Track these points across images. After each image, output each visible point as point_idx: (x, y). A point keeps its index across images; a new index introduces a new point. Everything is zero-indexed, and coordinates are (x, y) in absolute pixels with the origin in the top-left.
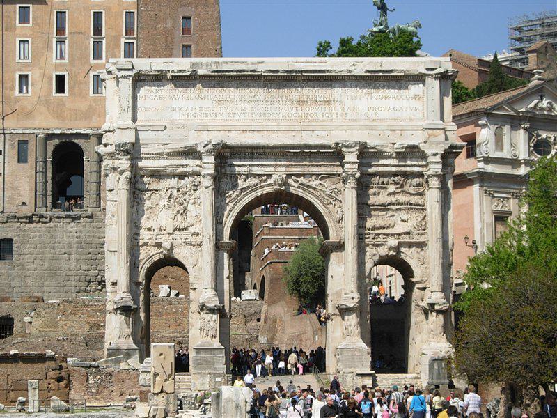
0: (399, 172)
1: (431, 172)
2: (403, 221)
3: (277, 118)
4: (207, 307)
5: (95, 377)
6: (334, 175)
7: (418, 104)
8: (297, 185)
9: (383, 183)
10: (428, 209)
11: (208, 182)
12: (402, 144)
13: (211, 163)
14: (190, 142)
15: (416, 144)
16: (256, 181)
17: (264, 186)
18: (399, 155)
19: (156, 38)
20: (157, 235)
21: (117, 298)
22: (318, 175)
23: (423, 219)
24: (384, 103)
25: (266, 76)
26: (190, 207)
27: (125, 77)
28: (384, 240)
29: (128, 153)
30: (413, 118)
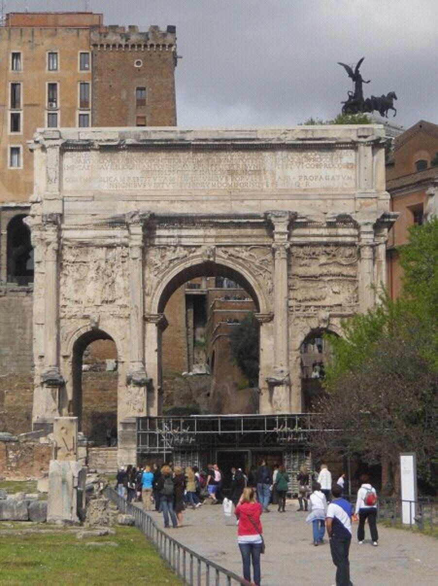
1: (363, 242)
2: (335, 293)
3: (206, 188)
4: (134, 381)
5: (15, 451)
7: (350, 173)
8: (226, 256)
9: (314, 253)
10: (360, 280)
11: (137, 253)
14: (119, 212)
15: (348, 214)
16: (186, 252)
17: (193, 257)
18: (330, 225)
19: (111, 110)
20: (85, 307)
21: (44, 372)
24: (315, 172)
25: (196, 145)
26: (119, 279)
27: (51, 147)
28: (315, 312)
29: (55, 224)
30: (345, 186)
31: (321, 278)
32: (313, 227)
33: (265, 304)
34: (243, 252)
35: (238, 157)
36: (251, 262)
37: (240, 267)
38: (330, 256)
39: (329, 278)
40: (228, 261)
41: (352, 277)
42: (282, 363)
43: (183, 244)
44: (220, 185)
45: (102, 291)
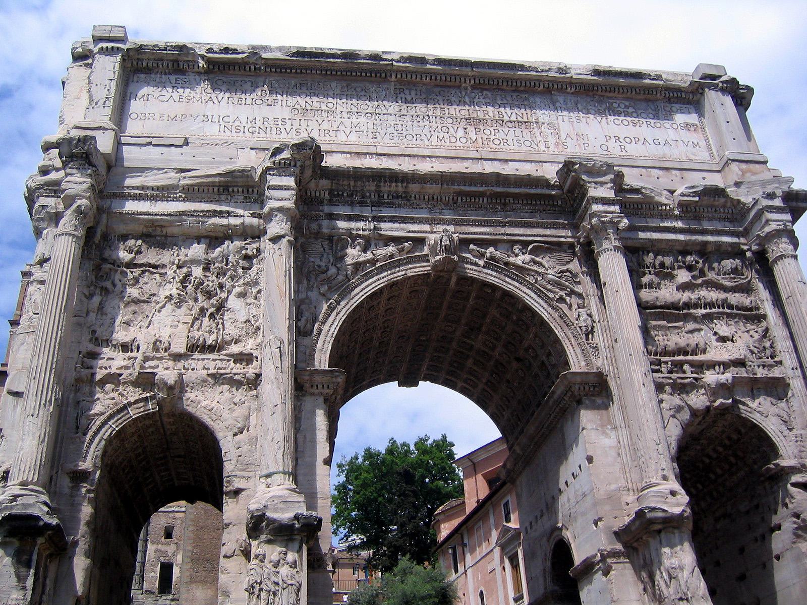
0: (694, 243)
1: (773, 226)
2: (723, 339)
6: (560, 244)
7: (694, 137)
8: (481, 263)
12: (693, 187)
13: (287, 188)
16: (391, 249)
17: (410, 260)
20: (146, 359)
22: (525, 244)
23: (765, 336)
26: (233, 302)
30: (693, 157)
31: (685, 311)
32: (652, 216)
33: (580, 356)
34: (516, 255)
35: (483, 101)
36: (536, 272)
37: (517, 284)
38: (696, 273)
39: (703, 311)
40: (486, 271)
41: (751, 309)
42: (665, 473)
43: (382, 232)
44: (453, 140)
45: (192, 326)
